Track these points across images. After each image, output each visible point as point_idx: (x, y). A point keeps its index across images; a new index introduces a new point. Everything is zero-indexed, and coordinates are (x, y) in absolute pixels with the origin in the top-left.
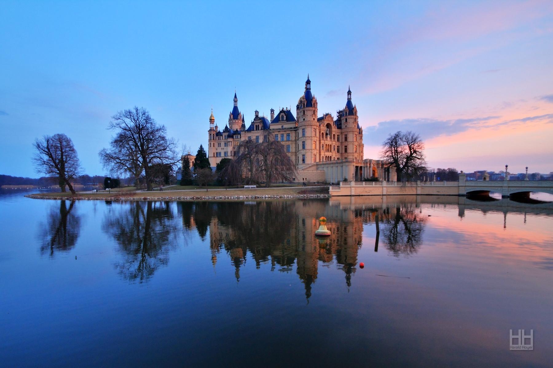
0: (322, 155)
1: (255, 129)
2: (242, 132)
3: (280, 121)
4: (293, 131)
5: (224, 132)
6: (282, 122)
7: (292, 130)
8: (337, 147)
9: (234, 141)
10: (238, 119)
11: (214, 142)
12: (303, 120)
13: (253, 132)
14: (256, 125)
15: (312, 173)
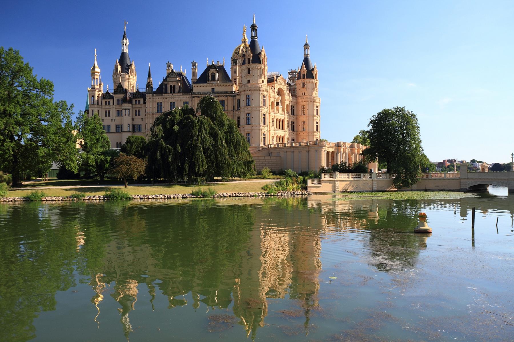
0: (272, 134)
1: (169, 90)
2: (146, 95)
3: (209, 81)
4: (230, 98)
5: (116, 92)
6: (212, 82)
7: (228, 95)
8: (292, 122)
9: (132, 107)
10: (130, 73)
11: (99, 109)
12: (247, 82)
13: (166, 95)
14: (171, 86)
15: (264, 161)
